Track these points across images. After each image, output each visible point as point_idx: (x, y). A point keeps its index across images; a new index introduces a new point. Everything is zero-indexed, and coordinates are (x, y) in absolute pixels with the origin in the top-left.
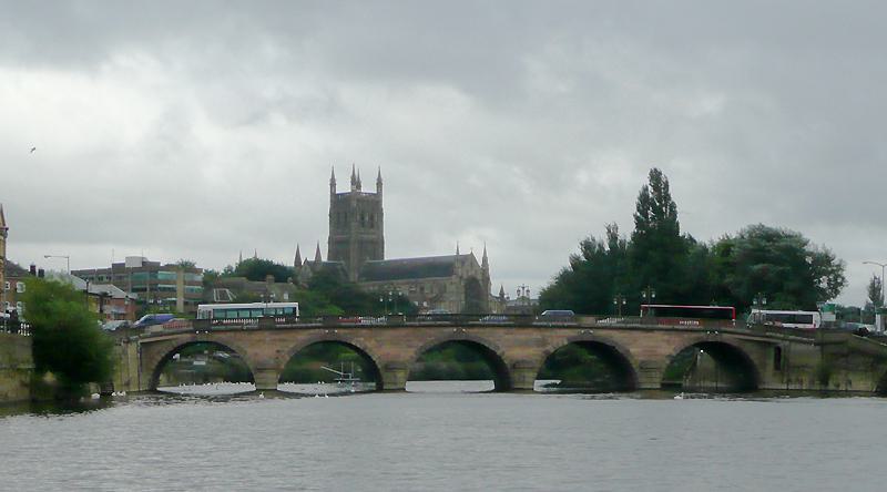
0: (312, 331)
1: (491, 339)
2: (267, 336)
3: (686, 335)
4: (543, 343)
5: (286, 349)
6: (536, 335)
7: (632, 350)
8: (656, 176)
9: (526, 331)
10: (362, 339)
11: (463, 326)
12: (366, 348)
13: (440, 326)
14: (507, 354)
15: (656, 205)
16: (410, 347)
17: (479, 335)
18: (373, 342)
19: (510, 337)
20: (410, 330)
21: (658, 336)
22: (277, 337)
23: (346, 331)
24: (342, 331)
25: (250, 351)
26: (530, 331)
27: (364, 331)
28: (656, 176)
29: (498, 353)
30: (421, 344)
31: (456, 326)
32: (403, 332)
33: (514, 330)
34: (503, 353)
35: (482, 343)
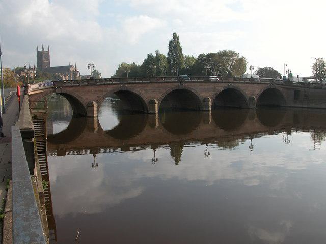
0: (114, 86)
2: (92, 88)
3: (264, 86)
4: (214, 89)
5: (102, 96)
6: (212, 86)
8: (175, 35)
10: (138, 89)
15: (175, 45)
16: (160, 93)
18: (144, 91)
19: (201, 87)
20: (161, 84)
22: (97, 89)
23: (131, 85)
24: (129, 85)
25: (84, 97)
26: (210, 84)
28: (175, 35)
30: (164, 91)
32: (157, 85)
33: (203, 83)
34: (199, 95)
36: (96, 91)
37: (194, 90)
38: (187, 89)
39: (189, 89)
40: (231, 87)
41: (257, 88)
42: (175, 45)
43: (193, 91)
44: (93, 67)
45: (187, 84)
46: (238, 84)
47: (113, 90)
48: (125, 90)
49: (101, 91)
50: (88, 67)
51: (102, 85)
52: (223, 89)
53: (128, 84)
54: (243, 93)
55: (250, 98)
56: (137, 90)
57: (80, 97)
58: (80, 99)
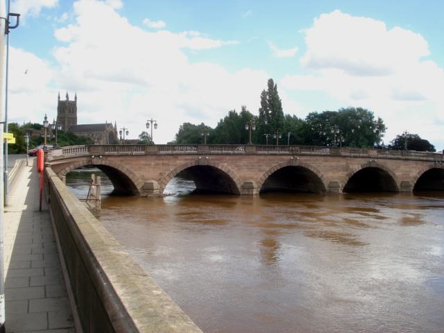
1: (314, 165)
3: (425, 164)
4: (346, 168)
5: (167, 173)
6: (343, 163)
7: (397, 174)
8: (271, 83)
9: (338, 159)
10: (226, 164)
11: (297, 155)
12: (229, 171)
13: (281, 155)
14: (325, 176)
15: (271, 100)
16: (260, 171)
17: (308, 162)
19: (325, 163)
20: (262, 158)
21: (412, 164)
22: (160, 162)
23: (214, 157)
24: (211, 157)
27: (228, 157)
28: (271, 83)
29: (319, 175)
30: (268, 169)
31: (293, 155)
32: (256, 158)
33: (329, 158)
34: (322, 176)
35: (310, 168)
36: (157, 164)
37: (314, 168)
38: (303, 166)
39: (306, 167)
40: (373, 165)
41: (413, 167)
42: (271, 100)
43: (312, 170)
44: (156, 125)
45: (303, 158)
46: (385, 161)
47: (186, 164)
48: (206, 164)
49: (166, 164)
50: (148, 124)
51: (169, 155)
52: (360, 169)
53: (210, 154)
54: (391, 174)
55: (402, 182)
56: (225, 166)
57: (131, 173)
58: (130, 177)
